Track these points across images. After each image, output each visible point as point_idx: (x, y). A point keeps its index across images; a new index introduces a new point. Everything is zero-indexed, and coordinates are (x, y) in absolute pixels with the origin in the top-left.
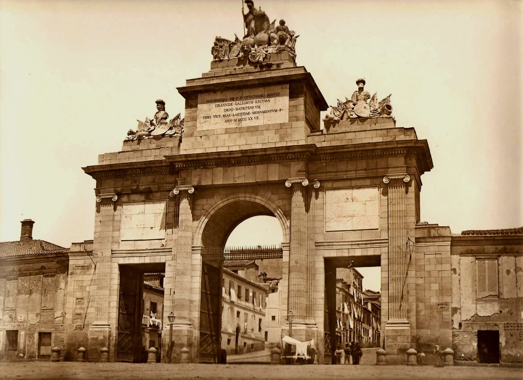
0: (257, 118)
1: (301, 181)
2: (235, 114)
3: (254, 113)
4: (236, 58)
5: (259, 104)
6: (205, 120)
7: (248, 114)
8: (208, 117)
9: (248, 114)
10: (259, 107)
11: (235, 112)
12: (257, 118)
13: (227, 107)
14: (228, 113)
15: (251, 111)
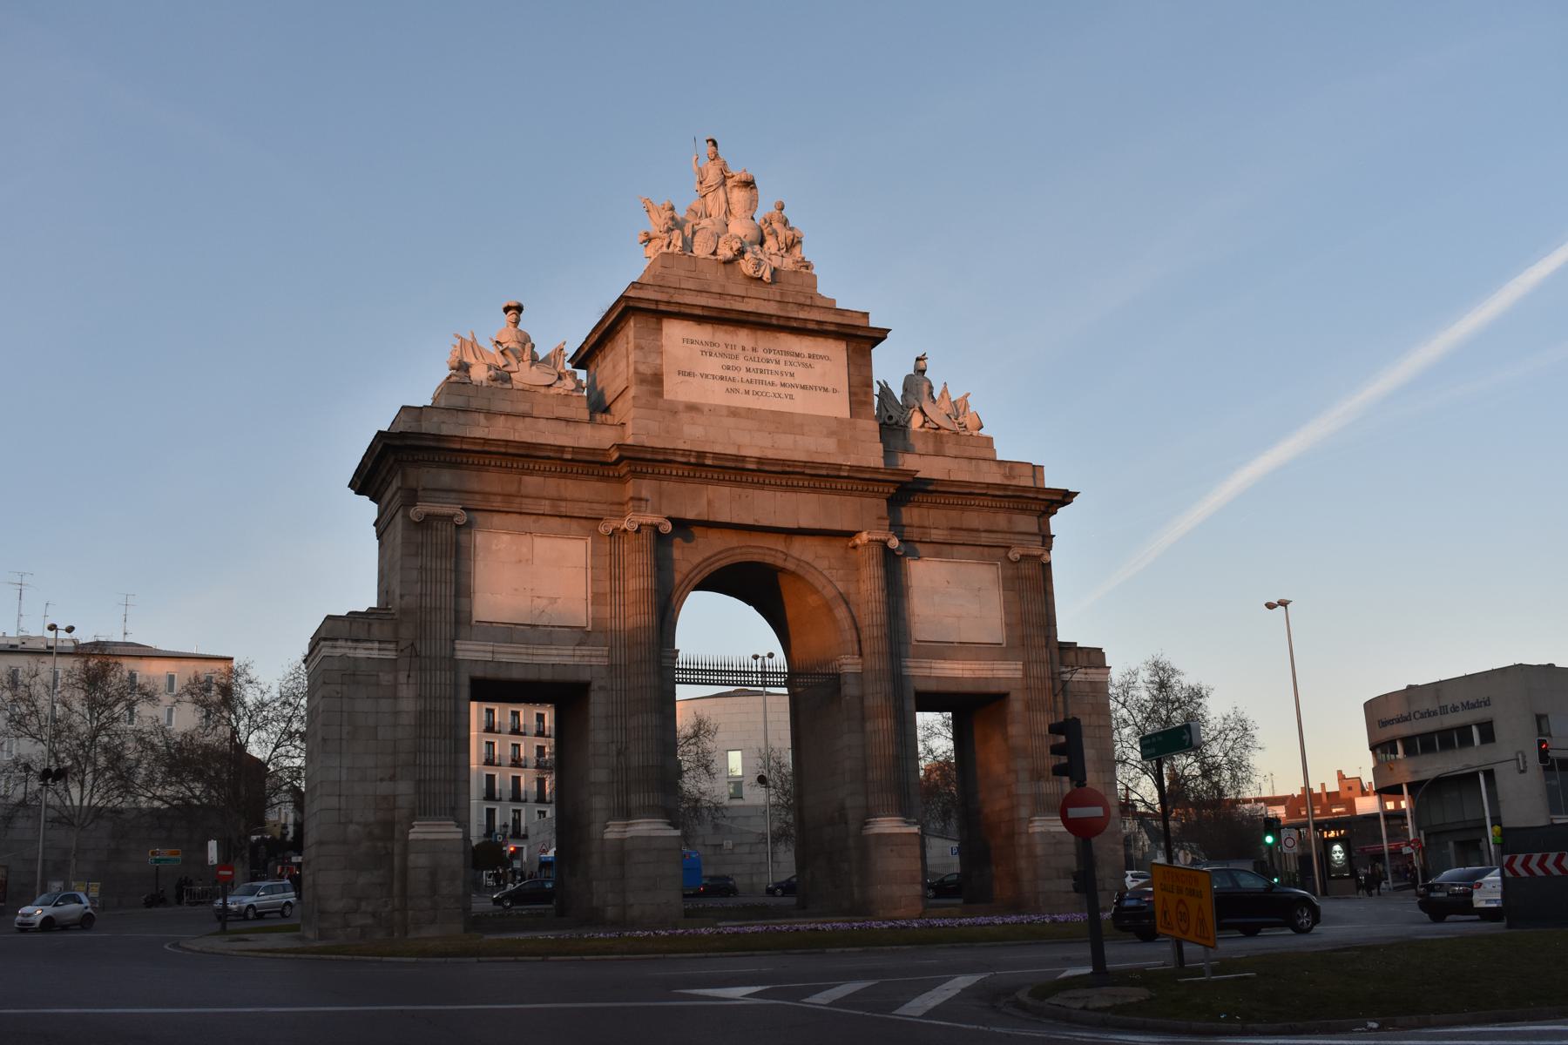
0: (791, 397)
1: (886, 538)
2: (745, 380)
3: (783, 385)
4: (713, 257)
5: (788, 369)
6: (681, 378)
7: (773, 384)
8: (689, 374)
9: (773, 384)
10: (792, 375)
11: (744, 374)
12: (791, 397)
13: (730, 363)
14: (730, 374)
15: (776, 379)
